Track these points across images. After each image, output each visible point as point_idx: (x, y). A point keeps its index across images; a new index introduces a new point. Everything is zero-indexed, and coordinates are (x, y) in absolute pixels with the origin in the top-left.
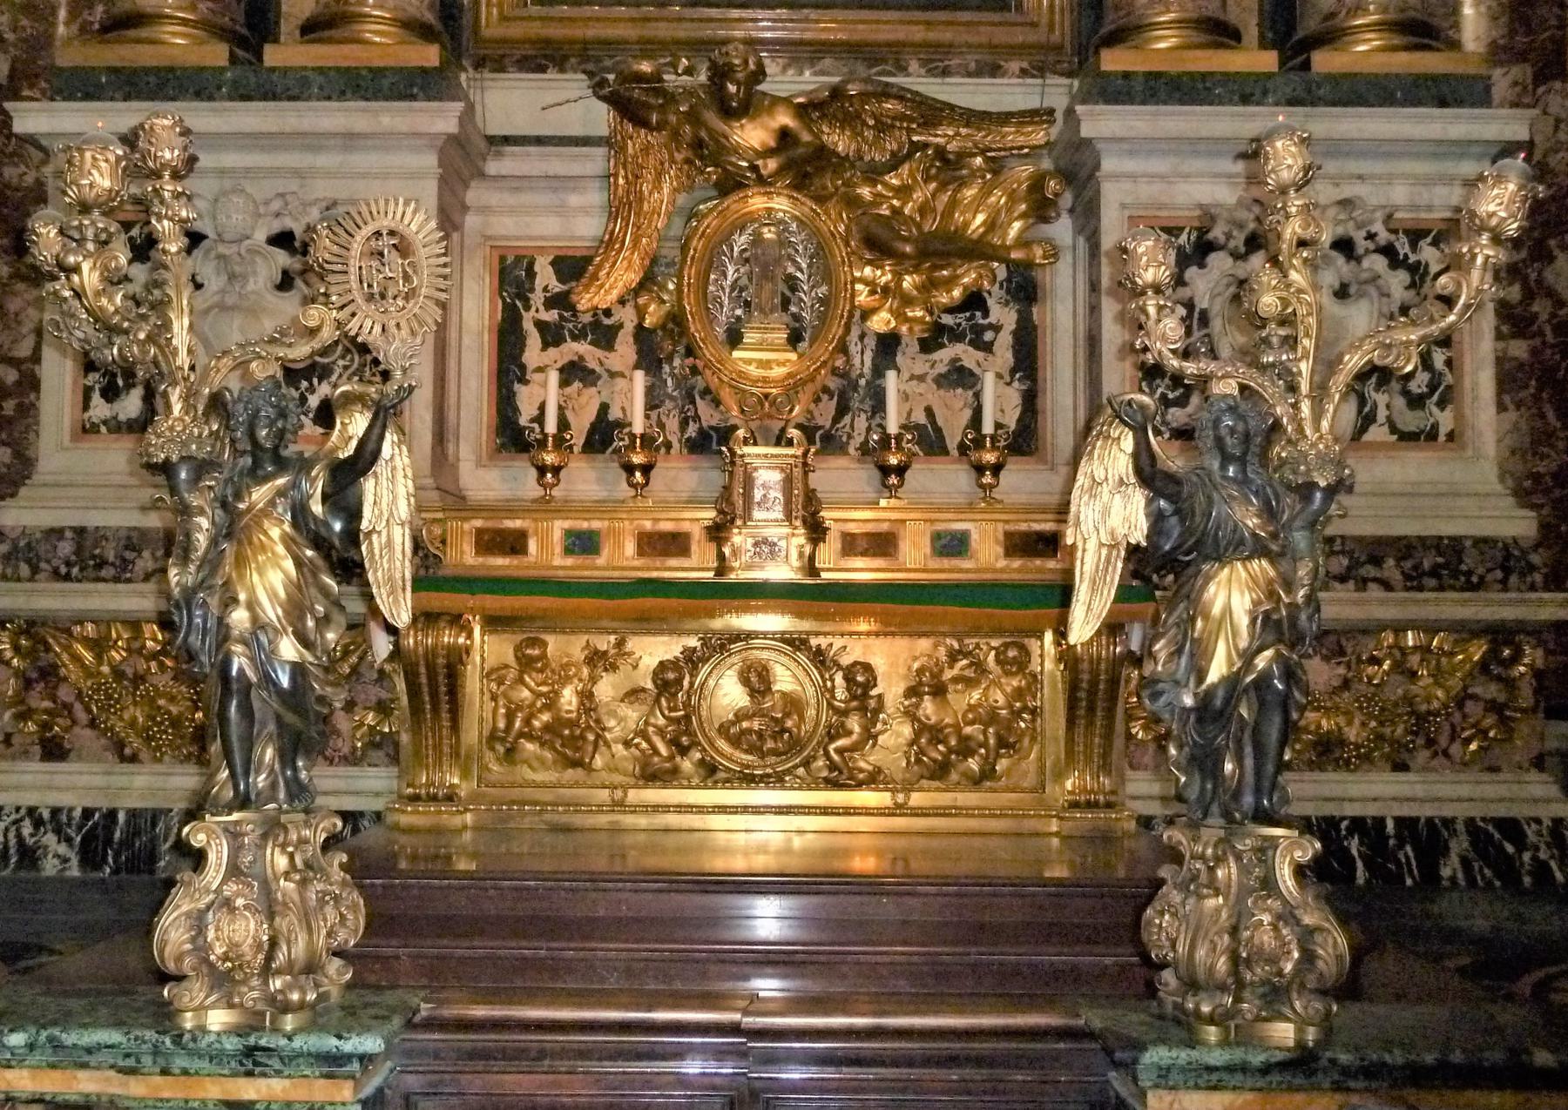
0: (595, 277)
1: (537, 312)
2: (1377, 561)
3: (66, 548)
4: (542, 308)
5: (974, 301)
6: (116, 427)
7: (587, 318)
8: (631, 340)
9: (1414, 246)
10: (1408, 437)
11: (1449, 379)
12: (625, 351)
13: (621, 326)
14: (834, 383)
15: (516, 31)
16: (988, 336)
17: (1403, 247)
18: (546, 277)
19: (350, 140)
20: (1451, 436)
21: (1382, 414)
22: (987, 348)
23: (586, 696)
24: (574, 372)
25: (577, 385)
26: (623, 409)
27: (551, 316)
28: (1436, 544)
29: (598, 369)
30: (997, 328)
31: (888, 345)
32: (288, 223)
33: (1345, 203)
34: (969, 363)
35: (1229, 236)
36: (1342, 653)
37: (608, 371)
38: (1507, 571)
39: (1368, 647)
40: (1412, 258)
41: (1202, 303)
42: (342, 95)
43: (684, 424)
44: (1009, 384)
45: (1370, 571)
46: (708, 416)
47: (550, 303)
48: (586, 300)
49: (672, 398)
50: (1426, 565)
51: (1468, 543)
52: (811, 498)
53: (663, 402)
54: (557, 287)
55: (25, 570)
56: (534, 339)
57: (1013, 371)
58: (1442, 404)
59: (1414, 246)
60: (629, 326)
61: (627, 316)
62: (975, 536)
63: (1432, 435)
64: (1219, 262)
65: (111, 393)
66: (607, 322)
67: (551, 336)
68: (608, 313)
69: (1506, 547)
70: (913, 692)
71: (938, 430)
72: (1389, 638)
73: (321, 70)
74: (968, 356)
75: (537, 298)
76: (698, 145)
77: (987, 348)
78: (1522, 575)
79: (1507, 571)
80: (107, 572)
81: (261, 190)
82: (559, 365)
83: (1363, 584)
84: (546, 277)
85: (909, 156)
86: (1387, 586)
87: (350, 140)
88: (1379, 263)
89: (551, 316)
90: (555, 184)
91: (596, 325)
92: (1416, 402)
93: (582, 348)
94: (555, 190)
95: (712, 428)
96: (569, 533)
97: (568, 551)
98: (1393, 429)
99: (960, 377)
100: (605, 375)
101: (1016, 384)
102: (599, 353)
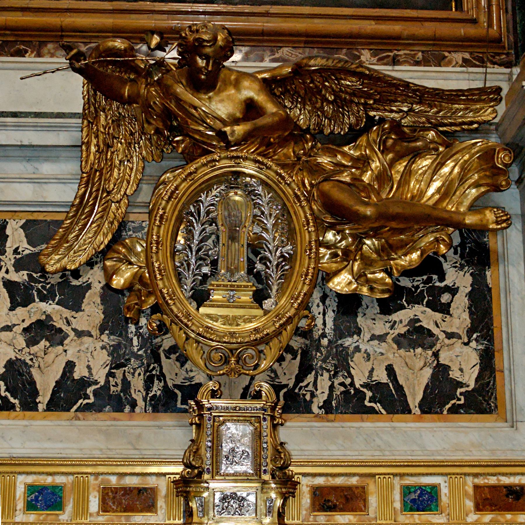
0: (64, 239)
4: (11, 269)
5: (431, 265)
7: (55, 279)
8: (99, 300)
12: (92, 312)
13: (89, 287)
16: (445, 298)
24: (42, 331)
25: (44, 343)
26: (89, 367)
27: (20, 277)
29: (65, 328)
30: (453, 291)
31: (349, 304)
34: (427, 324)
37: (74, 330)
43: (149, 383)
44: (466, 344)
46: (173, 372)
47: (19, 266)
49: (138, 357)
52: (279, 449)
53: (129, 360)
57: (470, 332)
60: (97, 287)
61: (95, 277)
62: (444, 490)
66: (75, 283)
68: (76, 273)
71: (399, 388)
74: (428, 318)
76: (167, 115)
82: (26, 325)
85: (367, 129)
90: (29, 153)
91: (64, 284)
93: (50, 308)
94: (29, 160)
95: (175, 386)
96: (31, 488)
99: (417, 337)
100: (72, 334)
101: (473, 344)
102: (67, 313)
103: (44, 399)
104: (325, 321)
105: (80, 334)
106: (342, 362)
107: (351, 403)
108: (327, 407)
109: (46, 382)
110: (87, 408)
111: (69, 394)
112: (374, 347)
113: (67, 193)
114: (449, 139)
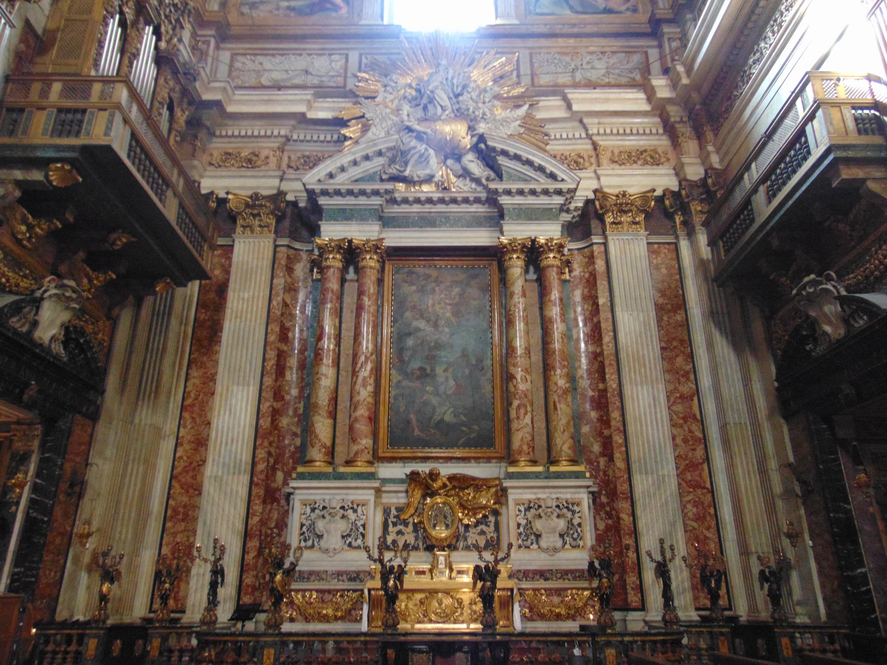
1: (392, 519)
5: (485, 516)
6: (306, 547)
10: (573, 547)
12: (411, 528)
17: (570, 506)
22: (489, 526)
23: (406, 605)
24: (400, 533)
27: (395, 520)
32: (343, 504)
33: (558, 498)
39: (565, 593)
41: (530, 519)
46: (429, 543)
47: (394, 517)
48: (402, 517)
54: (396, 513)
56: (391, 525)
61: (411, 520)
63: (579, 546)
64: (533, 511)
65: (305, 540)
67: (395, 524)
70: (470, 604)
72: (569, 592)
73: (351, 473)
74: (483, 527)
75: (392, 516)
77: (489, 526)
81: (339, 497)
83: (564, 580)
84: (394, 512)
87: (357, 488)
88: (565, 511)
89: (395, 520)
92: (575, 540)
93: (401, 527)
99: (482, 533)
104: (462, 529)
106: (466, 539)
114: (489, 487)
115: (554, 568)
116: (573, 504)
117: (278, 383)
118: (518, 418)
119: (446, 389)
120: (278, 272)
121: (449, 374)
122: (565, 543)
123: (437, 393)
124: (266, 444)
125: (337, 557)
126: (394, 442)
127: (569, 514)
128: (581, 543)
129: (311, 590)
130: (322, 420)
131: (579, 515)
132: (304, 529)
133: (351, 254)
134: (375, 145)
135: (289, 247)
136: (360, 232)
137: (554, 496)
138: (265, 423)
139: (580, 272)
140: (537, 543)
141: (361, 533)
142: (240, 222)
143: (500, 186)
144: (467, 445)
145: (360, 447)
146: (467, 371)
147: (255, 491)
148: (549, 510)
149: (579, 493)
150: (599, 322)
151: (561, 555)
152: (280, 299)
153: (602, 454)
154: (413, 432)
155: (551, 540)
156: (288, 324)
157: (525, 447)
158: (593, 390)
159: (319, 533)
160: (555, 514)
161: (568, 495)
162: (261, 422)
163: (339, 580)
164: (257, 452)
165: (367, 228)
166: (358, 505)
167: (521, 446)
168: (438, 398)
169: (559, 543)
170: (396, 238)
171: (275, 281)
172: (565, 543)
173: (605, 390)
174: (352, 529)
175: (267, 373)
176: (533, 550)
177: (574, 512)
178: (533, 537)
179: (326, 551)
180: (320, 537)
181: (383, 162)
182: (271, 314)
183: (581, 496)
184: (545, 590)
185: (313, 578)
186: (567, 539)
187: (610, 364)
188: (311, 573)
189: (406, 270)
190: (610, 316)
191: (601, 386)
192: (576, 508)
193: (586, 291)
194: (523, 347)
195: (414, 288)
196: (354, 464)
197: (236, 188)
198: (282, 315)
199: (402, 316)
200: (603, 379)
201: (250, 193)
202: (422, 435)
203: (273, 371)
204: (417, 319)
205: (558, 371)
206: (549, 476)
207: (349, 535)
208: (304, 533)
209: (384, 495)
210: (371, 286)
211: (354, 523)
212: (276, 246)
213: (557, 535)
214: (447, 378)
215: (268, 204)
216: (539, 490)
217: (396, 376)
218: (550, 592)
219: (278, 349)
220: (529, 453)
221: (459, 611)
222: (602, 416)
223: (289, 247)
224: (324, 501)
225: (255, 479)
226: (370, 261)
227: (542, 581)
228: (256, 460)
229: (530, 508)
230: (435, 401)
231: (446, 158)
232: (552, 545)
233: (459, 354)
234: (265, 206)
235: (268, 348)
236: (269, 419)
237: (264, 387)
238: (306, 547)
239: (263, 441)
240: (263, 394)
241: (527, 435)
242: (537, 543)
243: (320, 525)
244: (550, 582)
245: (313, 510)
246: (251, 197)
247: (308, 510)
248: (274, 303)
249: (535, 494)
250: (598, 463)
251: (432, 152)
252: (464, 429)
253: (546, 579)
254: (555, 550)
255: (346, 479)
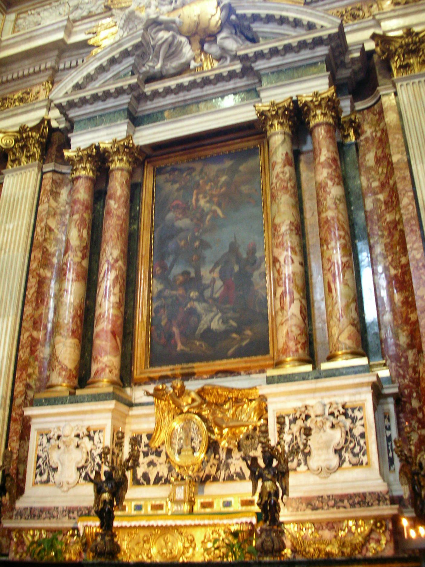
1: (143, 448)
2: (342, 501)
3: (28, 512)
6: (42, 483)
9: (353, 411)
10: (354, 465)
11: (365, 447)
14: (216, 462)
15: (143, 376)
17: (350, 412)
18: (145, 440)
19: (92, 412)
20: (367, 464)
21: (347, 459)
24: (151, 464)
25: (151, 467)
27: (146, 449)
28: (355, 495)
32: (78, 432)
33: (331, 404)
35: (301, 415)
36: (334, 528)
38: (379, 501)
40: (353, 415)
42: (92, 401)
45: (340, 504)
47: (145, 446)
50: (356, 501)
51: (367, 494)
55: (19, 517)
56: (141, 455)
58: (364, 455)
59: (353, 411)
64: (300, 423)
67: (146, 454)
69: (378, 494)
73: (88, 395)
75: (143, 445)
78: (384, 502)
79: (379, 501)
80: (36, 518)
81: (73, 424)
83: (338, 508)
84: (145, 440)
86: (345, 507)
87: (92, 412)
88: (342, 418)
91: (156, 451)
92: (355, 455)
97: (135, 510)
98: (350, 463)
103: (152, 481)
105: (161, 464)
106: (228, 466)
107: (230, 478)
108: (224, 480)
109: (152, 478)
110: (162, 484)
111: (158, 480)
112: (236, 462)
113: (153, 426)
114: (251, 401)
115: (324, 493)
116: (353, 410)
117: (39, 312)
118: (282, 308)
119: (212, 292)
120: (43, 199)
121: (216, 275)
122: (342, 461)
123: (201, 299)
124: (24, 376)
125: (71, 492)
126: (155, 360)
127: (348, 422)
128: (365, 459)
129: (40, 530)
130: (63, 340)
131: (362, 422)
132: (40, 462)
133: (100, 159)
134: (120, 46)
135: (54, 171)
136: (106, 136)
137: (326, 401)
138: (24, 354)
139: (372, 133)
140: (306, 463)
141: (98, 464)
142: (11, 157)
143: (251, 50)
144: (238, 354)
145: (100, 366)
146: (236, 268)
147: (13, 426)
148: (319, 419)
149: (360, 393)
150: (395, 183)
151: (339, 476)
152: (43, 224)
153: (411, 346)
154: (176, 346)
155: (323, 457)
156: (52, 250)
157: (292, 344)
158: (395, 268)
159: (54, 466)
160: (329, 424)
161: (346, 398)
162: (21, 353)
163: (70, 518)
164: (16, 385)
165: (115, 130)
166: (95, 432)
167: (286, 344)
168: (204, 305)
169: (335, 461)
170: (148, 135)
171: (40, 208)
172: (342, 461)
173: (408, 264)
174: (87, 461)
175: (28, 302)
176: (301, 472)
177: (354, 420)
178: (300, 456)
179: (60, 486)
180: (55, 470)
181: (133, 62)
182: (35, 241)
183: (363, 397)
184: (313, 523)
185: (44, 515)
186: (347, 455)
187: (412, 230)
188: (42, 510)
189: (169, 169)
190: (408, 173)
191: (403, 260)
192: (358, 414)
193: (380, 151)
194: (287, 222)
195: (177, 186)
196: (96, 385)
197: (9, 127)
198: (45, 240)
199: (163, 219)
200: (404, 251)
201: (17, 129)
202: (187, 349)
203: (34, 299)
204: (180, 219)
205: (332, 244)
206: (319, 375)
207: (83, 467)
208: (40, 466)
209: (132, 420)
210: (119, 188)
211: (90, 453)
212: (43, 174)
213: (331, 451)
214: (214, 281)
215: (34, 134)
216: (307, 396)
217: (157, 286)
218: (318, 525)
219: (39, 275)
220: (297, 351)
221: (191, 550)
222: (407, 298)
223: (54, 171)
224: (59, 428)
225: (13, 414)
226: (119, 165)
227: (309, 511)
228: (15, 393)
229: (296, 419)
230: (199, 307)
231: (202, 43)
232: (324, 465)
233: (227, 250)
234: (32, 137)
235: (30, 276)
236: (28, 350)
237: (24, 317)
238: (42, 483)
239: (22, 374)
240: (24, 324)
241: (294, 329)
242: (306, 463)
243: (55, 458)
244: (320, 511)
245: (49, 440)
246: (19, 132)
247: (45, 440)
248: (38, 229)
249: (301, 400)
250: (406, 358)
251: (183, 39)
252: (234, 335)
253: (315, 509)
254: (330, 471)
255: (82, 402)
